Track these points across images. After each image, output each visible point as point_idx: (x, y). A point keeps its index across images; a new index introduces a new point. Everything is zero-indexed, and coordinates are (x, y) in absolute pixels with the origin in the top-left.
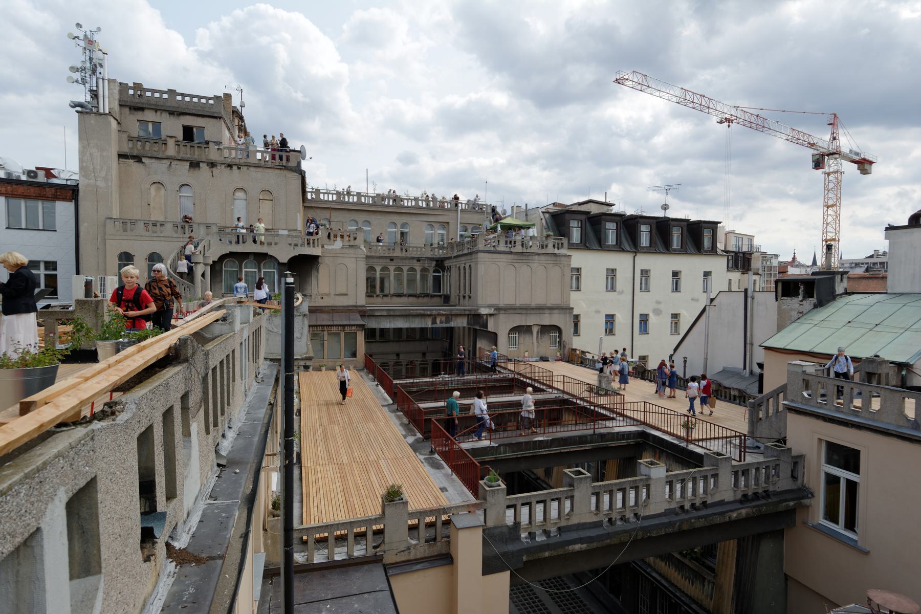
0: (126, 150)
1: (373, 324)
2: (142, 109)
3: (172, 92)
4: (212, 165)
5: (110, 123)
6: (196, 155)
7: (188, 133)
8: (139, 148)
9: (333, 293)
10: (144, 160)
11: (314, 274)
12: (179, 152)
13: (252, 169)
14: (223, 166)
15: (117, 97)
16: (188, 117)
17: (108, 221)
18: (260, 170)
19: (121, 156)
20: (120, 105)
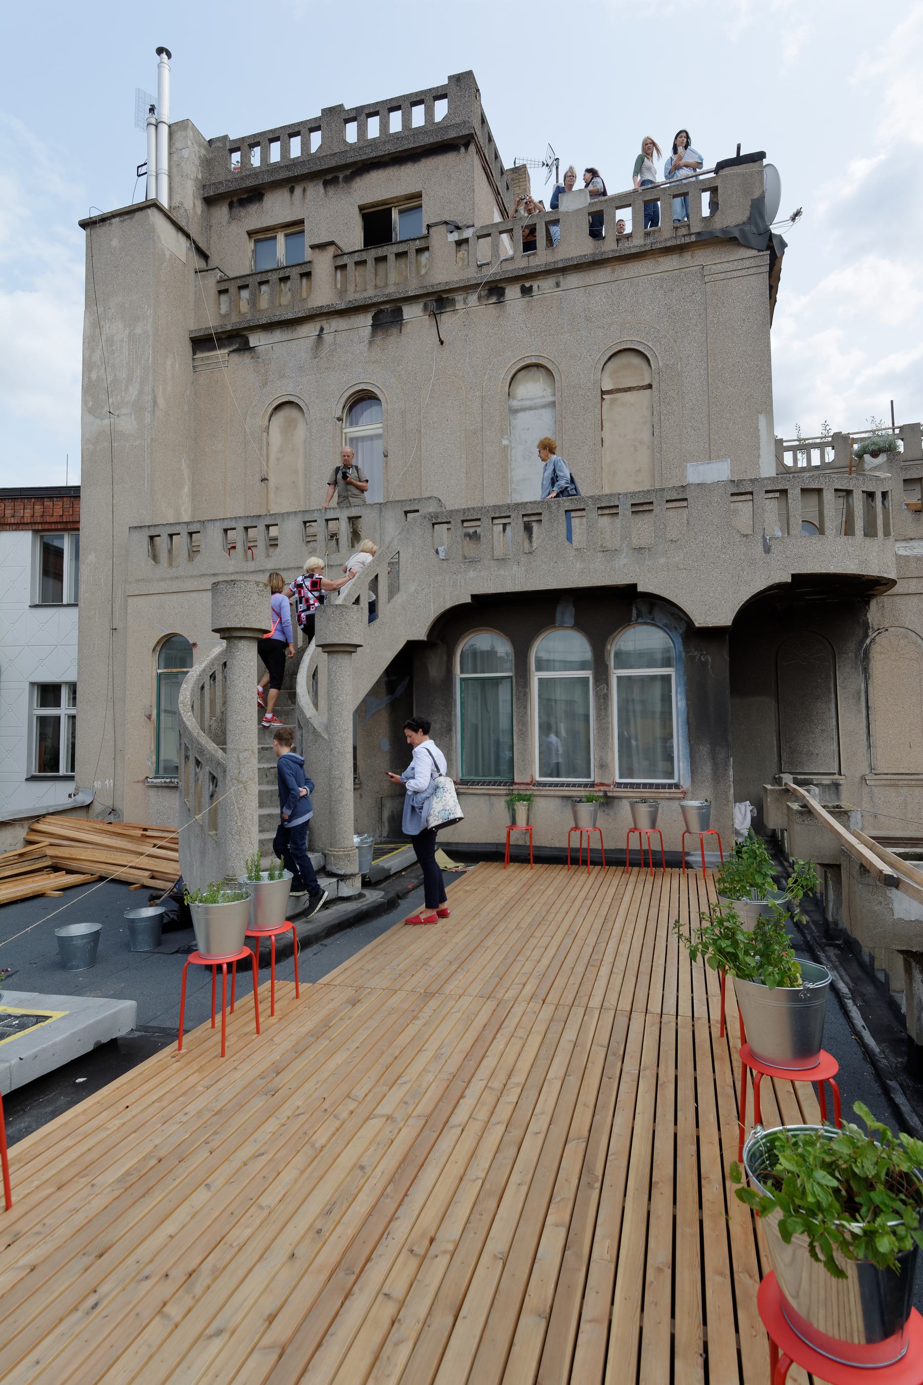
0: (210, 322)
3: (336, 116)
4: (439, 301)
5: (152, 231)
6: (395, 279)
7: (377, 224)
8: (244, 307)
11: (847, 682)
12: (342, 292)
13: (572, 280)
14: (473, 298)
15: (192, 170)
17: (136, 535)
18: (601, 275)
19: (202, 343)
20: (210, 201)
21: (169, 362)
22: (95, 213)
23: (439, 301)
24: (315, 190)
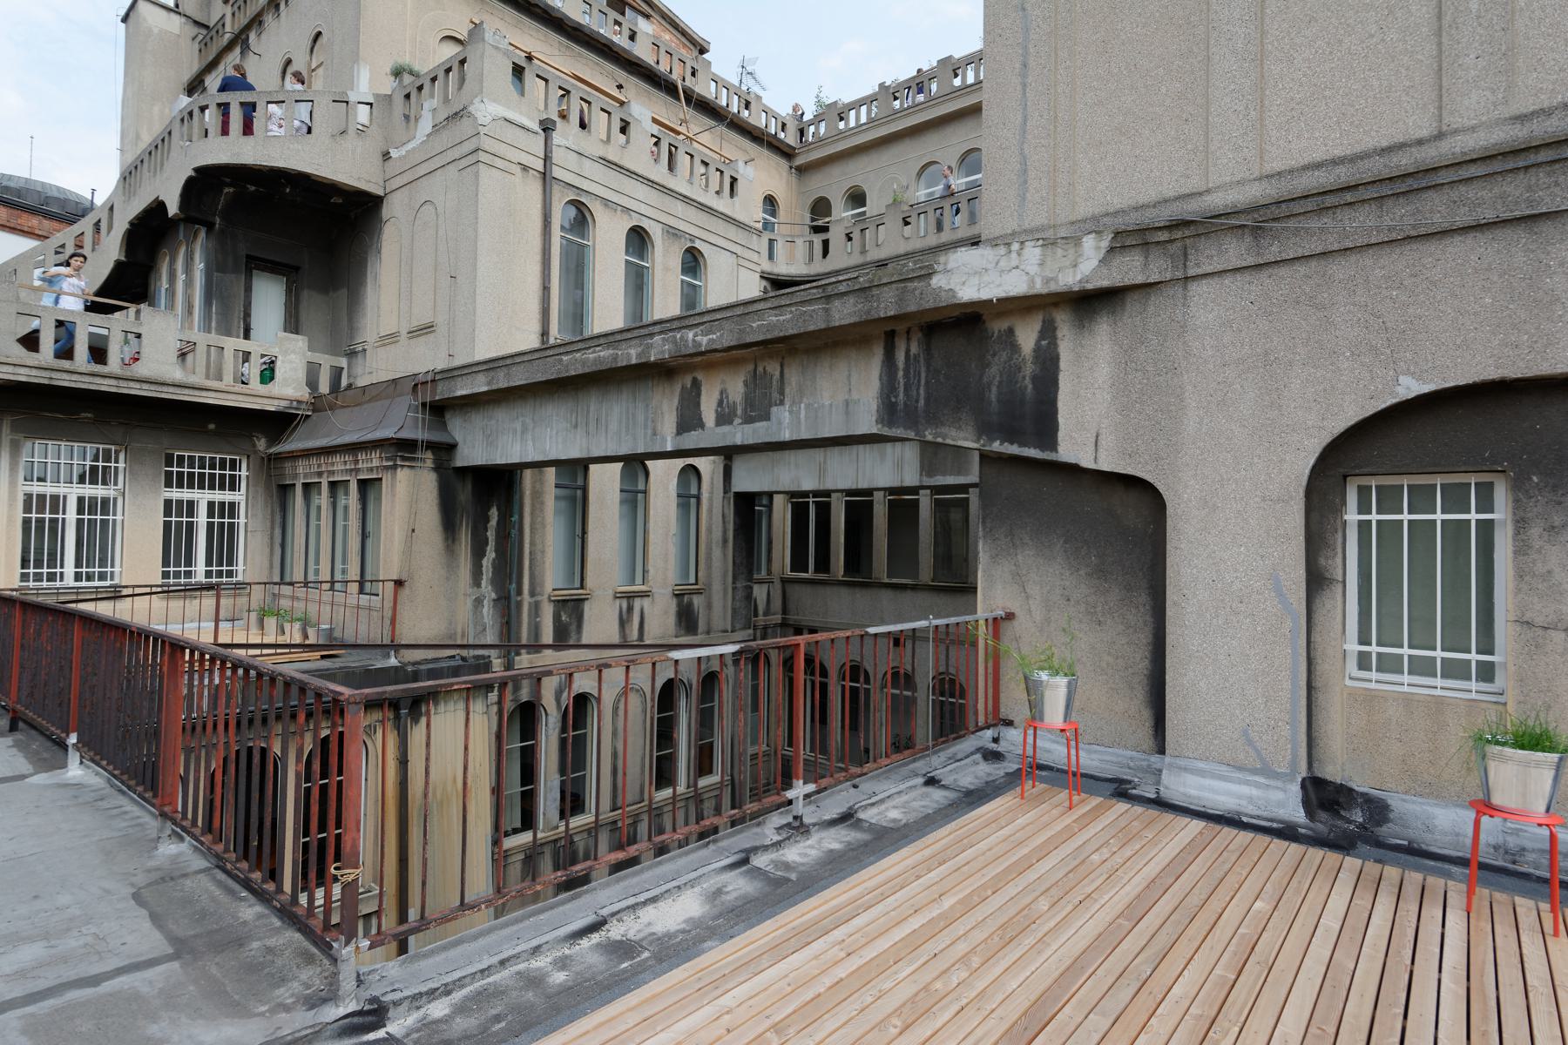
9: (404, 332)
21: (156, 109)
22: (123, 12)
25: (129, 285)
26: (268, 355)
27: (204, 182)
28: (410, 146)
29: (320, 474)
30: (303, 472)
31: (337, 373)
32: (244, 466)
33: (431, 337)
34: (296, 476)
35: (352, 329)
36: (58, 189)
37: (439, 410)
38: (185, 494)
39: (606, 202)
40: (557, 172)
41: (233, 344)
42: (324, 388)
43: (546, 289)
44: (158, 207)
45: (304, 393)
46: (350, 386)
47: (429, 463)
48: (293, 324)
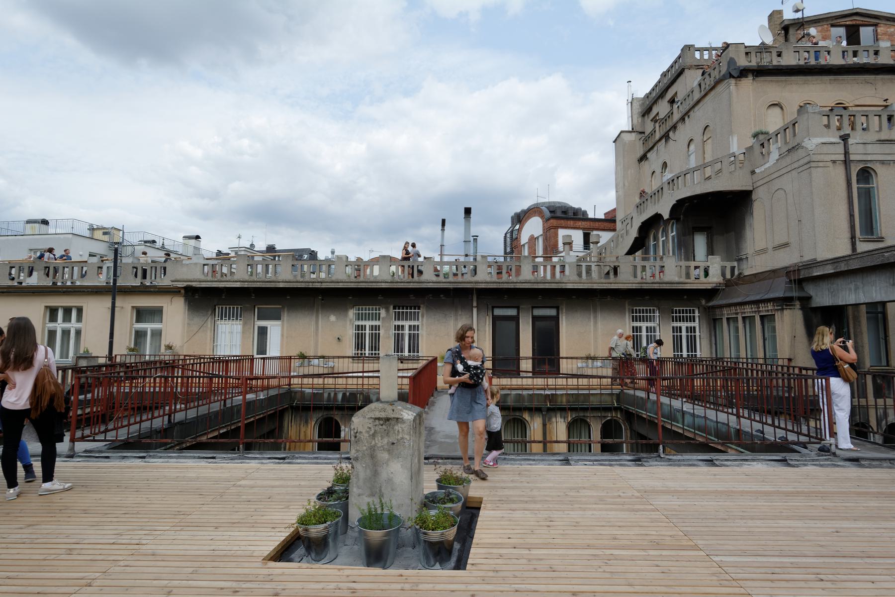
1: (823, 297)
2: (649, 110)
9: (770, 248)
10: (649, 155)
13: (696, 108)
16: (670, 90)
18: (701, 104)
23: (674, 127)
24: (660, 101)
25: (639, 245)
26: (707, 267)
27: (679, 207)
28: (767, 165)
29: (737, 314)
30: (726, 313)
31: (733, 269)
32: (697, 312)
33: (788, 249)
34: (722, 315)
35: (739, 249)
36: (559, 203)
37: (800, 283)
38: (678, 324)
39: (882, 162)
40: (852, 157)
41: (693, 264)
42: (728, 276)
43: (852, 216)
44: (657, 217)
45: (720, 279)
46: (740, 274)
47: (798, 306)
48: (711, 251)
